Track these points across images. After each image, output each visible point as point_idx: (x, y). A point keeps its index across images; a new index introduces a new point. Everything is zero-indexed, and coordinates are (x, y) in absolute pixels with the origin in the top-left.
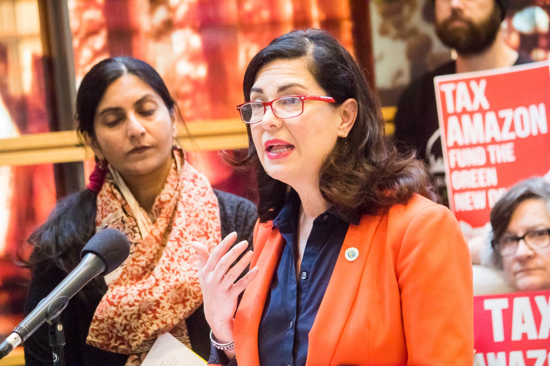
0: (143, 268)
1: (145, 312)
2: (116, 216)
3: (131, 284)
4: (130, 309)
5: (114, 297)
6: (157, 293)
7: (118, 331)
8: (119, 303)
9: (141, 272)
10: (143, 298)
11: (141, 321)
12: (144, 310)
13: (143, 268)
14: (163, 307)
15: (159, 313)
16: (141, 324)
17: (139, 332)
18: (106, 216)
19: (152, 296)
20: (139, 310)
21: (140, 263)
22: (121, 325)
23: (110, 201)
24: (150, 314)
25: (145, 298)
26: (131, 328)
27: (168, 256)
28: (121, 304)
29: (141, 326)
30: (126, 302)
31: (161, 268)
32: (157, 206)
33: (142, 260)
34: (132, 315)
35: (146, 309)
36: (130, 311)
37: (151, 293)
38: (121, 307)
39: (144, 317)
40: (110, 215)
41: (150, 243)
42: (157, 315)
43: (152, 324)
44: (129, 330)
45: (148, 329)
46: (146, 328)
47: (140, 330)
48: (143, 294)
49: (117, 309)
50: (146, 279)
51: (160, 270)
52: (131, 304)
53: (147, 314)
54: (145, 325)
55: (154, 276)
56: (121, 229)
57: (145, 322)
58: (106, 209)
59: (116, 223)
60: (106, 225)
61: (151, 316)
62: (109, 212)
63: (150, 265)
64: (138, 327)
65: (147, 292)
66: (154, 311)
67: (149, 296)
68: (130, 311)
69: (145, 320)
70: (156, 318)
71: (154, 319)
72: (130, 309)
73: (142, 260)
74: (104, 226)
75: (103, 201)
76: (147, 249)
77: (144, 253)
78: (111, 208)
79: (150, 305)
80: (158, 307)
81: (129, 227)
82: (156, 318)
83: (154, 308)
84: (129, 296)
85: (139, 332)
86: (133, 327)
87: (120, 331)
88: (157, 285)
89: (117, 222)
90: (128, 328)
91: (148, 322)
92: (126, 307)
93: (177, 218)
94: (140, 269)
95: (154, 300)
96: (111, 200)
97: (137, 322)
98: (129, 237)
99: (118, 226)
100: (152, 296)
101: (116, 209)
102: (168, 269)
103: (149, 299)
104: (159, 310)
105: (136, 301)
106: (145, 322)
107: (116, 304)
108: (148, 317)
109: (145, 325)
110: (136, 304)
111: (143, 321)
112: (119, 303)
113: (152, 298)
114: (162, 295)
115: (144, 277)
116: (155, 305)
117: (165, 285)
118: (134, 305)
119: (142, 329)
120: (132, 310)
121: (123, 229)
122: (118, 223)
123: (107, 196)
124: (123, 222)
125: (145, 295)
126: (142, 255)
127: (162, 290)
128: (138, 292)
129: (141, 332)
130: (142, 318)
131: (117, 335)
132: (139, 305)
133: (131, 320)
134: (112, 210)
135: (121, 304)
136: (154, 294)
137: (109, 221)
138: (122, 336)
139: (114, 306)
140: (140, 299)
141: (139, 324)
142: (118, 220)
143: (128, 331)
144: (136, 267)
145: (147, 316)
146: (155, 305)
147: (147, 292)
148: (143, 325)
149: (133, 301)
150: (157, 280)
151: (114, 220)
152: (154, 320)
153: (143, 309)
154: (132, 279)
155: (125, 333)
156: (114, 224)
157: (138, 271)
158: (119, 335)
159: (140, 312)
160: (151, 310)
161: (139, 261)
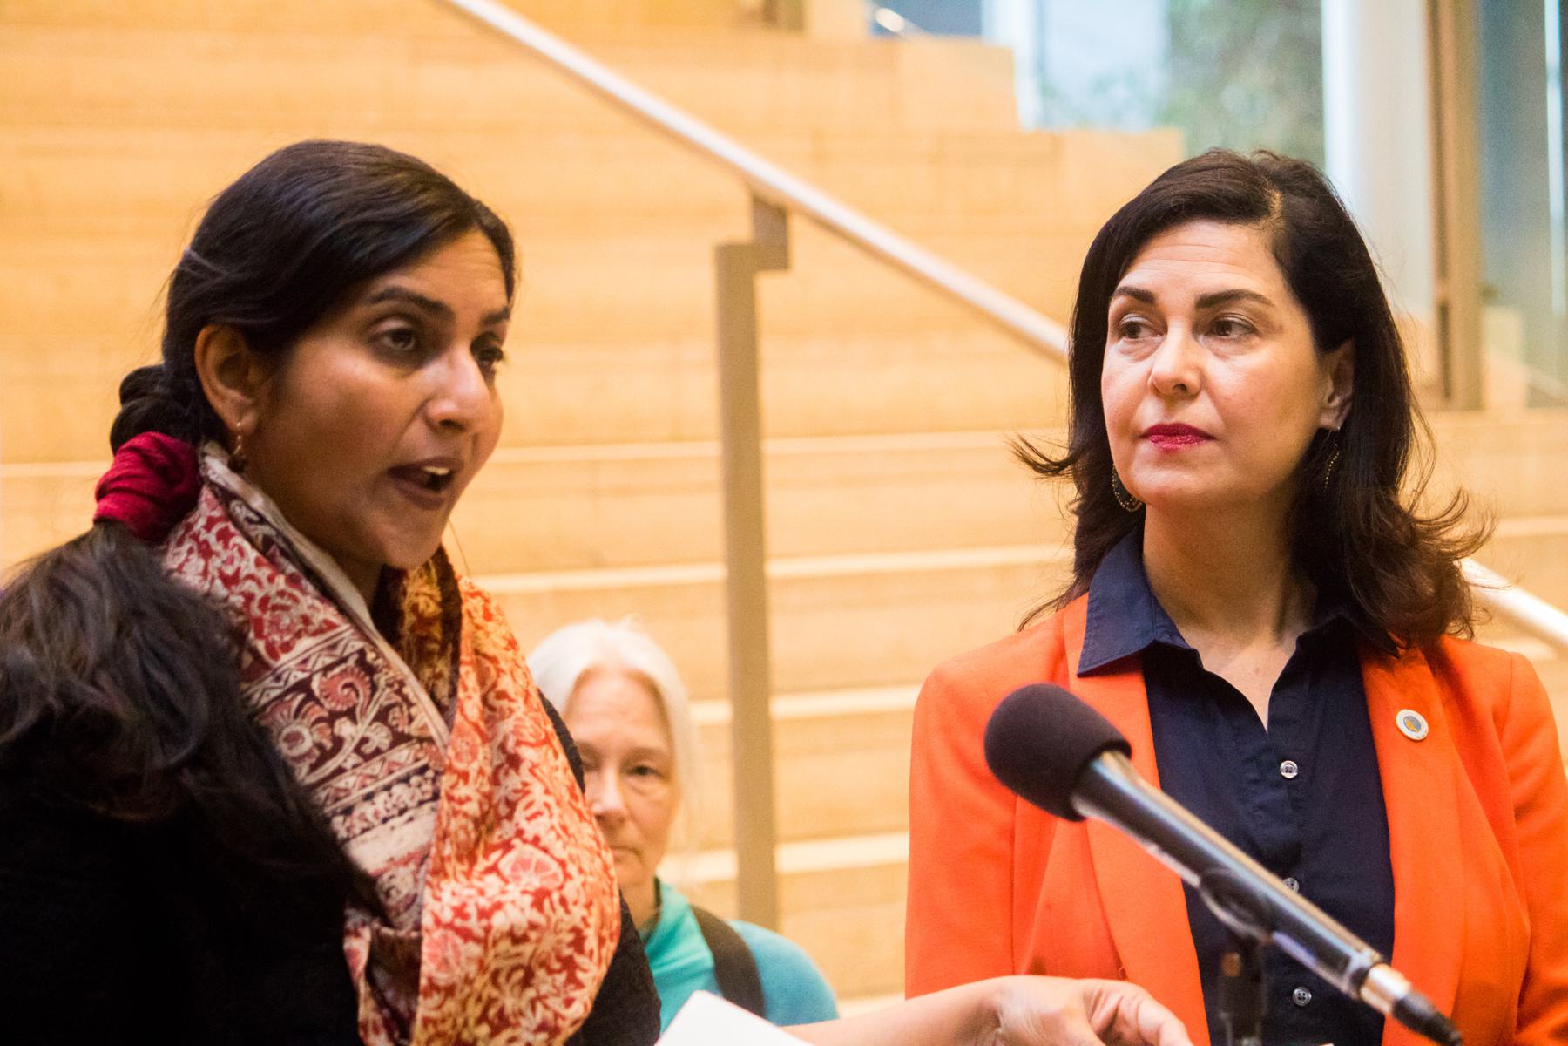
0: (478, 822)
1: (544, 964)
2: (333, 647)
3: (468, 875)
4: (514, 950)
5: (460, 912)
6: (575, 903)
7: (465, 1024)
8: (488, 930)
9: (473, 836)
10: (548, 919)
11: (531, 993)
12: (544, 957)
13: (478, 822)
14: (592, 952)
15: (585, 971)
16: (533, 1003)
17: (527, 1029)
18: (287, 647)
19: (568, 911)
20: (532, 957)
21: (467, 807)
22: (479, 999)
23: (296, 600)
24: (559, 971)
25: (554, 919)
26: (501, 1013)
27: (547, 792)
28: (493, 932)
29: (533, 1009)
30: (506, 928)
31: (552, 828)
32: (412, 629)
33: (468, 799)
34: (515, 969)
35: (549, 955)
36: (511, 957)
37: (563, 901)
38: (495, 943)
39: (545, 983)
40: (305, 643)
41: (467, 744)
42: (580, 975)
43: (569, 1002)
44: (496, 1021)
45: (557, 1015)
46: (550, 1015)
47: (530, 1021)
48: (546, 903)
49: (486, 949)
50: (486, 856)
51: (552, 835)
52: (519, 933)
53: (550, 971)
54: (546, 1007)
55: (545, 850)
56: (364, 691)
57: (546, 997)
58: (275, 623)
59: (337, 670)
60: (301, 676)
61: (561, 978)
62: (298, 635)
63: (488, 812)
64: (521, 1013)
65: (555, 896)
66: (569, 965)
67: (560, 910)
68: (511, 957)
69: (544, 989)
70: (580, 985)
71: (572, 986)
72: (514, 950)
73: (468, 799)
74: (292, 681)
75: (249, 597)
76: (469, 763)
77: (464, 776)
78: (306, 620)
79: (559, 942)
80: (580, 950)
81: (390, 685)
82: (580, 985)
83: (567, 952)
84: (508, 907)
85: (527, 1029)
86: (509, 1010)
87: (471, 1022)
88: (567, 876)
89: (343, 667)
90: (492, 1012)
91: (553, 995)
92: (505, 945)
93: (499, 676)
94: (471, 826)
95: (569, 927)
96: (296, 593)
97: (520, 996)
98: (394, 718)
99: (348, 680)
100: (568, 911)
101: (331, 626)
102: (564, 828)
103: (562, 920)
104: (579, 959)
105: (533, 926)
106: (546, 997)
107: (480, 933)
108: (554, 980)
109: (546, 1007)
110: (533, 935)
111: (538, 991)
112: (488, 930)
113: (567, 918)
114: (584, 912)
115: (480, 852)
116: (570, 944)
117: (582, 878)
118: (524, 939)
119: (539, 1019)
120: (518, 955)
121: (369, 692)
122: (344, 672)
123: (271, 579)
124: (370, 670)
125: (553, 909)
126: (461, 782)
127: (583, 900)
128: (528, 899)
129: (534, 1027)
130: (535, 981)
131: (459, 1035)
132: (539, 941)
133: (507, 988)
134: (311, 628)
135: (494, 934)
136: (571, 907)
137: (305, 662)
138: (470, 1040)
139: (477, 940)
140: (540, 919)
141: (524, 1004)
142: (343, 660)
143: (491, 1024)
144: (463, 821)
145: (549, 979)
146: (570, 944)
147: (555, 896)
148: (539, 1007)
149: (525, 925)
150: (562, 864)
151: (329, 661)
152: (572, 990)
153: (543, 952)
154: (460, 858)
155: (484, 1030)
156: (330, 674)
157: (467, 833)
158: (465, 1036)
159: (533, 964)
160: (559, 958)
161: (461, 802)
